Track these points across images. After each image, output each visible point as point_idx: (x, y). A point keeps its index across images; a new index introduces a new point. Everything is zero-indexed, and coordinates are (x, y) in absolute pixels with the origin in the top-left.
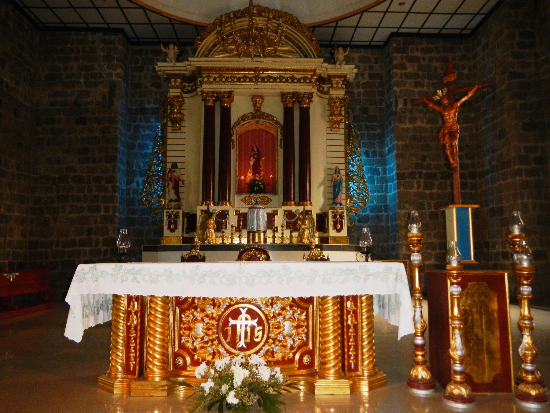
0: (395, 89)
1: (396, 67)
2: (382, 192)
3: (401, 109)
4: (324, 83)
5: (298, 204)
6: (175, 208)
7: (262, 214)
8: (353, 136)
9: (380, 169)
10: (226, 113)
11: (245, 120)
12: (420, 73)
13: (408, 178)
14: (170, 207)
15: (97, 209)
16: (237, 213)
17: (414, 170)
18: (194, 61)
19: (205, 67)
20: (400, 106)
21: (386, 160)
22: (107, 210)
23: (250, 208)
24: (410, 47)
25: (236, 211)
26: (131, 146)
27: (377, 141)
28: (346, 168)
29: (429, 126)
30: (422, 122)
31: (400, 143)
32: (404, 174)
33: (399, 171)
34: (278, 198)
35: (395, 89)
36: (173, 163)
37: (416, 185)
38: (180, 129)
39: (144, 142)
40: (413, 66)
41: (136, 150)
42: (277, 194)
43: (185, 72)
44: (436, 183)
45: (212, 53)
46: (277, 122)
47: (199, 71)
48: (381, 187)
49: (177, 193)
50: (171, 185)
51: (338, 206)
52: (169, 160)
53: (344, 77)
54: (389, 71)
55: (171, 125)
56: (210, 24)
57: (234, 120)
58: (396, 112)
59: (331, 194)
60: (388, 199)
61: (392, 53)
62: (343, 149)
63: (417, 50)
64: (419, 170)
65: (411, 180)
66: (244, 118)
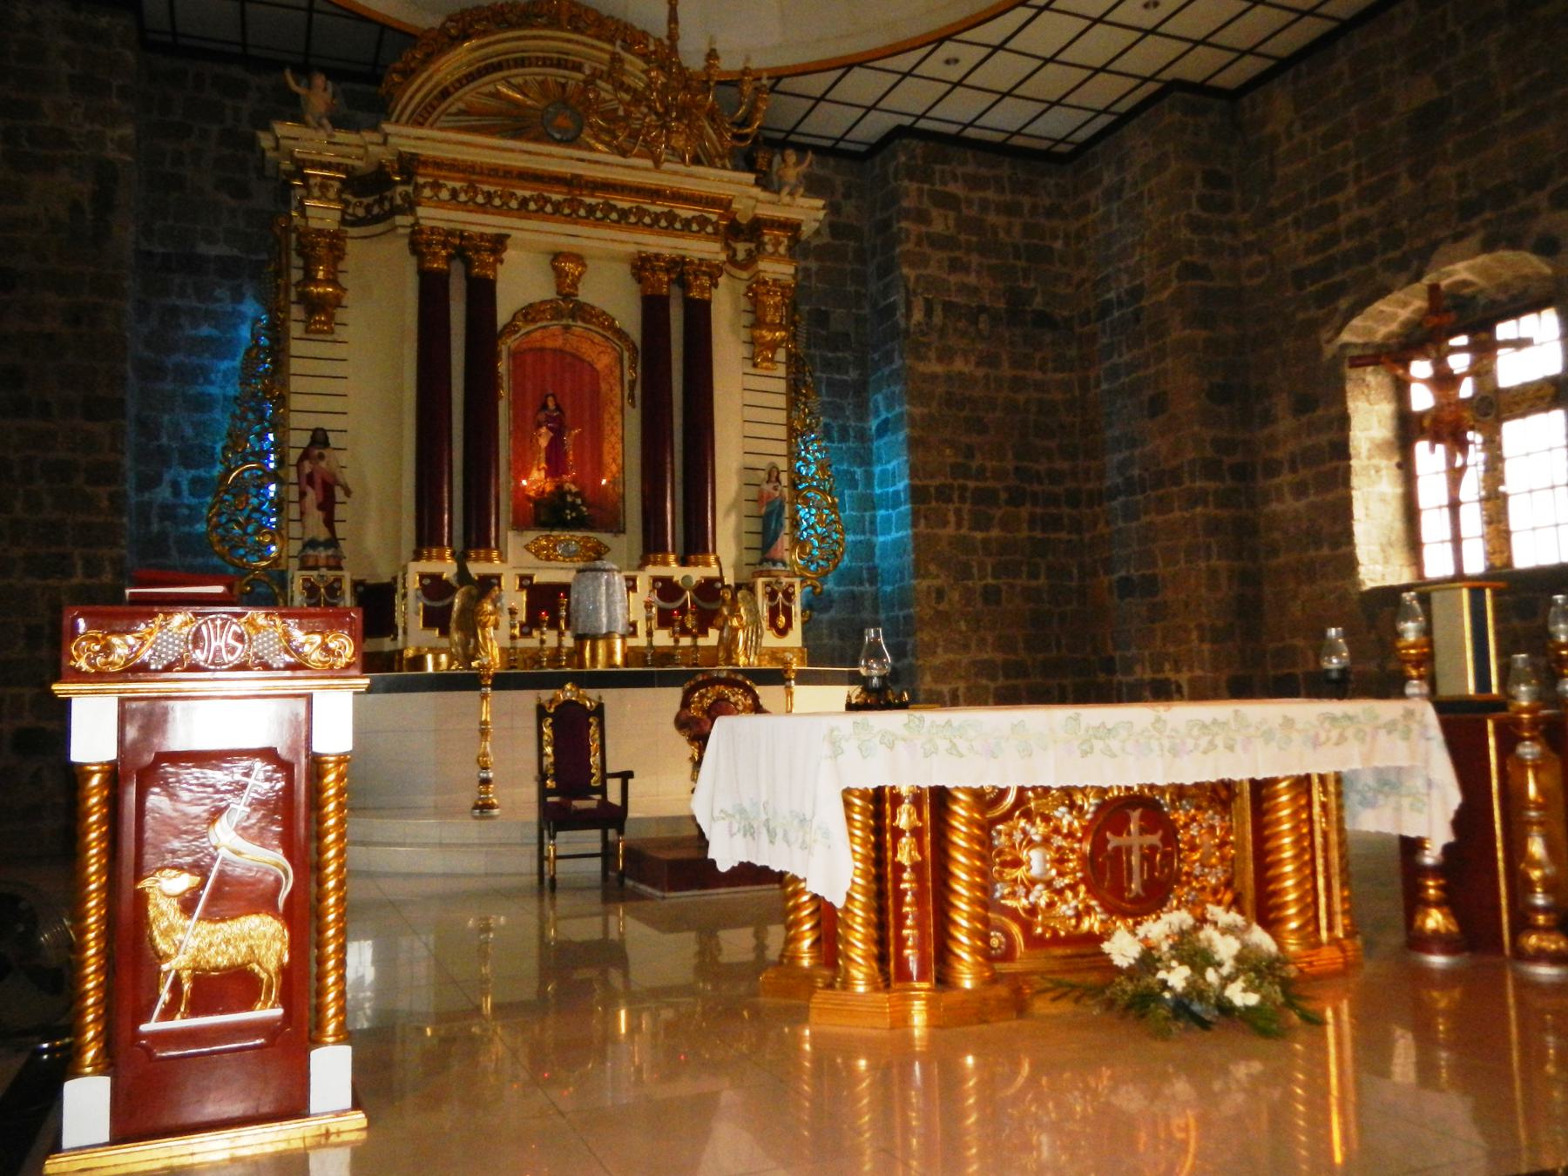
0: (905, 270)
1: (905, 214)
2: (863, 533)
3: (919, 324)
4: (736, 237)
5: (684, 562)
6: (329, 568)
8: (805, 384)
9: (859, 472)
10: (482, 294)
11: (534, 321)
12: (962, 237)
13: (937, 500)
14: (311, 562)
16: (526, 583)
17: (950, 481)
18: (401, 136)
19: (464, 161)
20: (918, 316)
21: (871, 450)
22: (92, 567)
23: (579, 571)
24: (938, 167)
25: (522, 578)
27: (850, 401)
28: (792, 470)
29: (980, 373)
30: (967, 362)
31: (918, 411)
32: (926, 488)
33: (918, 482)
35: (905, 270)
36: (316, 431)
37: (952, 518)
38: (332, 332)
39: (195, 360)
40: (946, 218)
41: (168, 386)
42: (623, 532)
43: (358, 163)
44: (998, 513)
45: (435, 115)
46: (620, 334)
47: (409, 165)
48: (861, 520)
49: (329, 522)
50: (312, 497)
51: (780, 567)
52: (295, 420)
53: (792, 227)
54: (885, 226)
55: (302, 316)
56: (431, 29)
57: (503, 317)
58: (907, 332)
59: (756, 536)
60: (877, 552)
61: (896, 179)
62: (782, 417)
63: (955, 177)
64: (961, 481)
65: (944, 506)
66: (529, 313)
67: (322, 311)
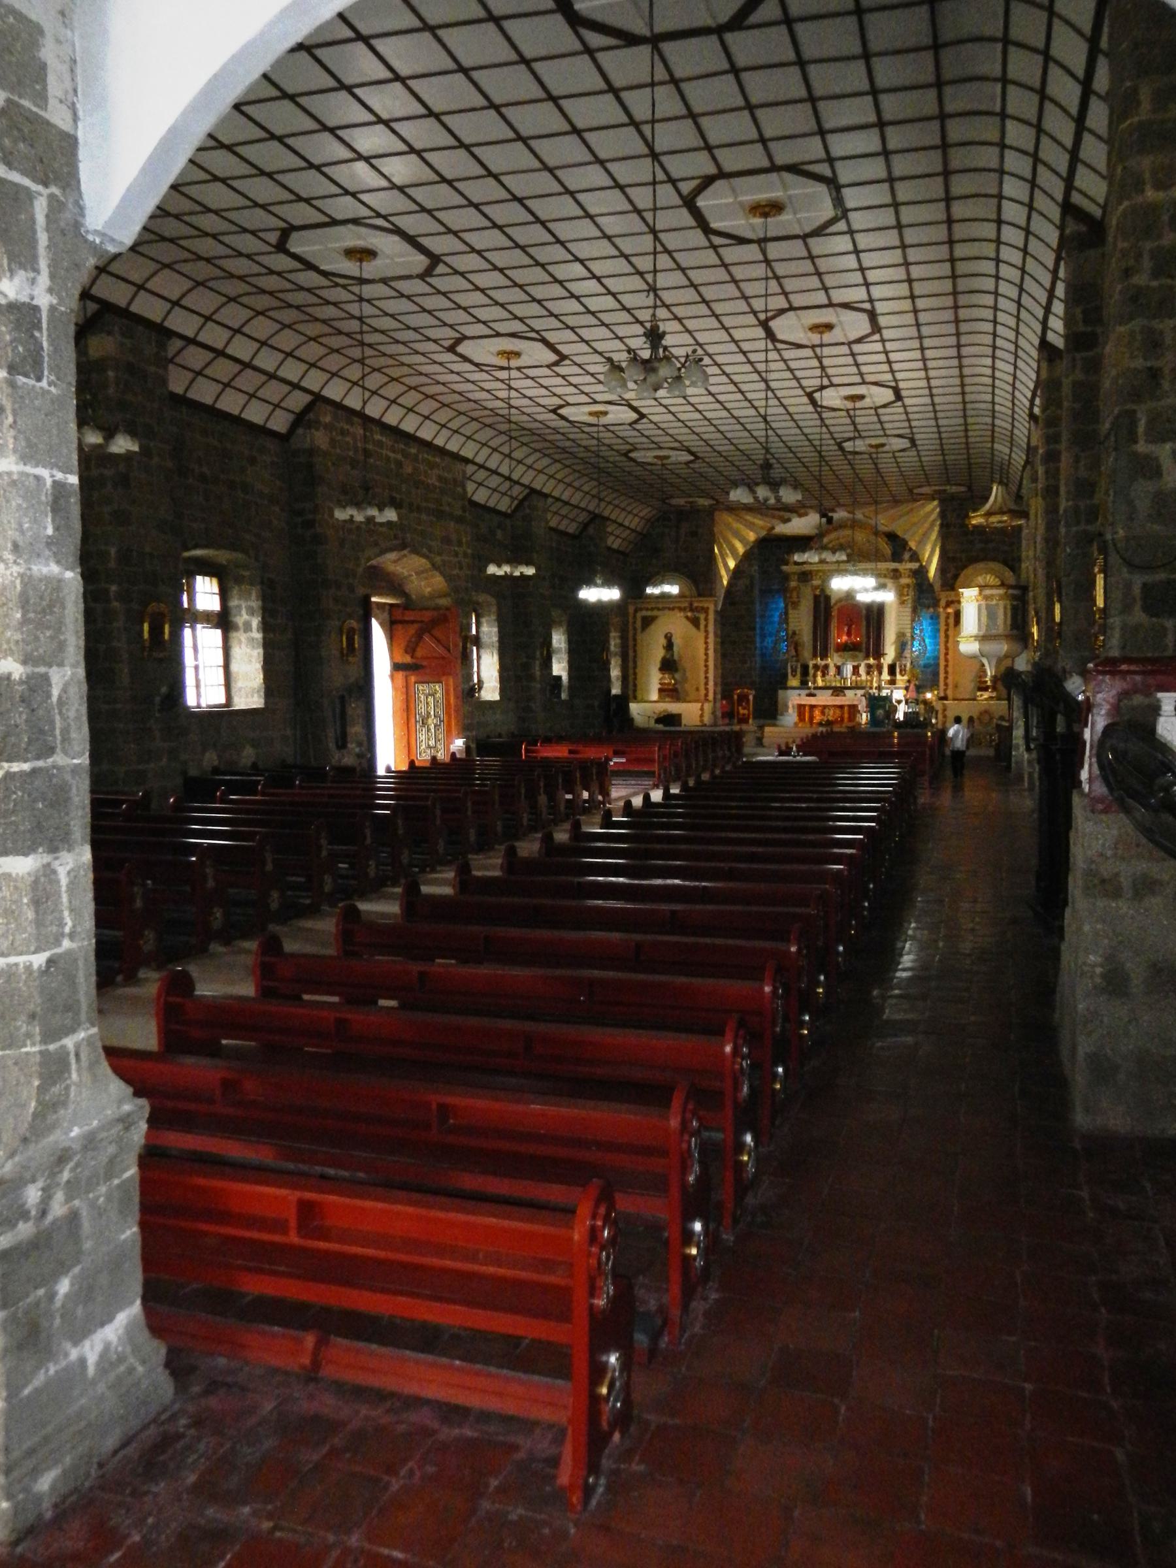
7: (848, 669)
15: (745, 662)
26: (762, 616)
34: (861, 655)
49: (796, 651)
67: (796, 605)
